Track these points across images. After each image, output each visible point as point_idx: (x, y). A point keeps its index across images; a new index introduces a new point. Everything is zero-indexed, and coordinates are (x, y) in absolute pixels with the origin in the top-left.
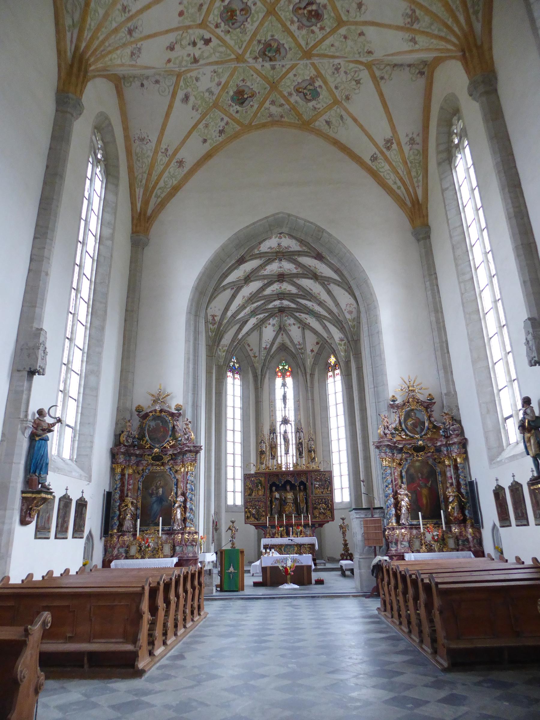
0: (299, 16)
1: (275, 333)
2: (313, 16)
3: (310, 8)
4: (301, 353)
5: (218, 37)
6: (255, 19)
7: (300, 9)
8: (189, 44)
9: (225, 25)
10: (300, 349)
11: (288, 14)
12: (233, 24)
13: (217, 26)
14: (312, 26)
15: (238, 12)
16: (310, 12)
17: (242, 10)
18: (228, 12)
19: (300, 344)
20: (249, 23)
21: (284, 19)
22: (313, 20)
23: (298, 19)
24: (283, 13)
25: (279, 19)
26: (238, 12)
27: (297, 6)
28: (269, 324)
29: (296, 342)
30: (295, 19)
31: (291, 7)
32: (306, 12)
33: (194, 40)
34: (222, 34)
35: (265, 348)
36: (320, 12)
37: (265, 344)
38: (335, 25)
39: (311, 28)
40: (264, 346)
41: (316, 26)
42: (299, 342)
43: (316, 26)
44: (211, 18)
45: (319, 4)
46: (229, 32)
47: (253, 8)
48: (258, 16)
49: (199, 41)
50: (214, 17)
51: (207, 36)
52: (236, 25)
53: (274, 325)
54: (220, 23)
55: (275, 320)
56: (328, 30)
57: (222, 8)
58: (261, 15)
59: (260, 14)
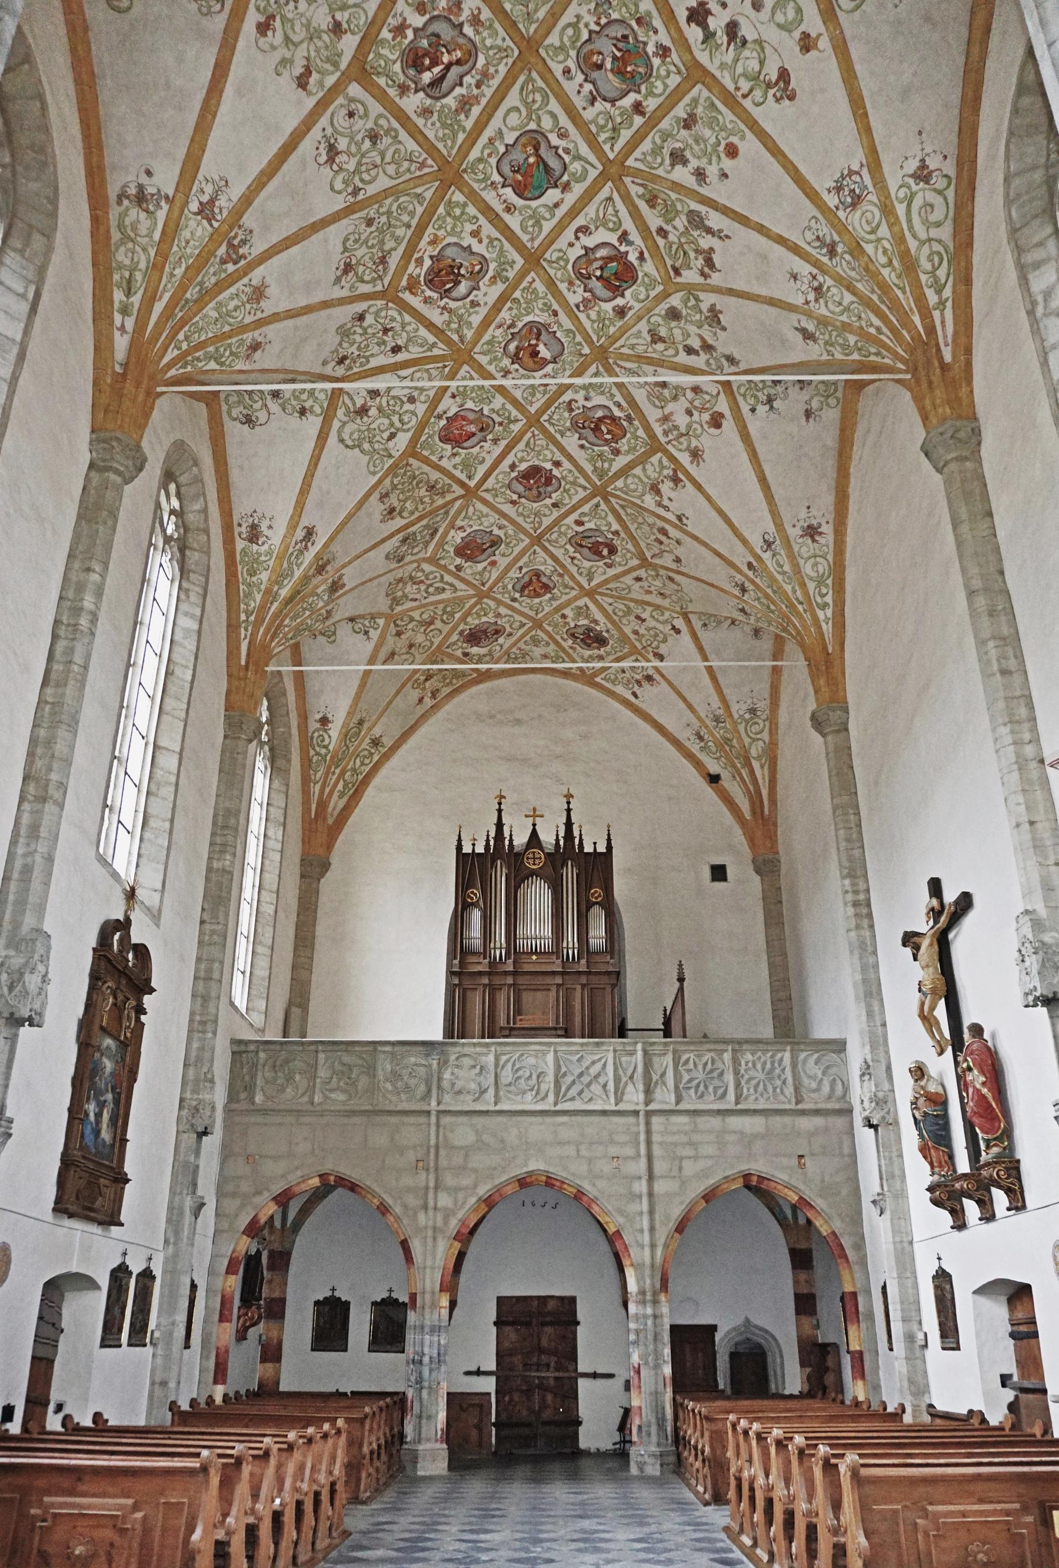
0: (461, 41)
2: (426, 54)
3: (437, 70)
5: (669, 17)
6: (570, 31)
7: (459, 62)
8: (744, 42)
9: (645, 44)
11: (488, 42)
12: (625, 37)
13: (664, 52)
14: (425, 25)
15: (609, 66)
16: (435, 62)
17: (599, 67)
18: (633, 75)
20: (587, 25)
21: (497, 25)
22: (425, 43)
23: (461, 33)
24: (499, 42)
25: (510, 24)
26: (609, 66)
27: (466, 67)
30: (468, 30)
31: (481, 61)
32: (446, 59)
33: (729, 44)
34: (657, 23)
36: (412, 72)
38: (371, 56)
39: (427, 16)
41: (416, 31)
43: (416, 31)
44: (674, 80)
45: (416, 91)
46: (639, 21)
47: (571, 64)
48: (561, 39)
49: (719, 33)
50: (667, 77)
51: (694, 33)
52: (618, 31)
54: (655, 54)
56: (385, 34)
57: (643, 88)
58: (553, 39)
59: (557, 44)
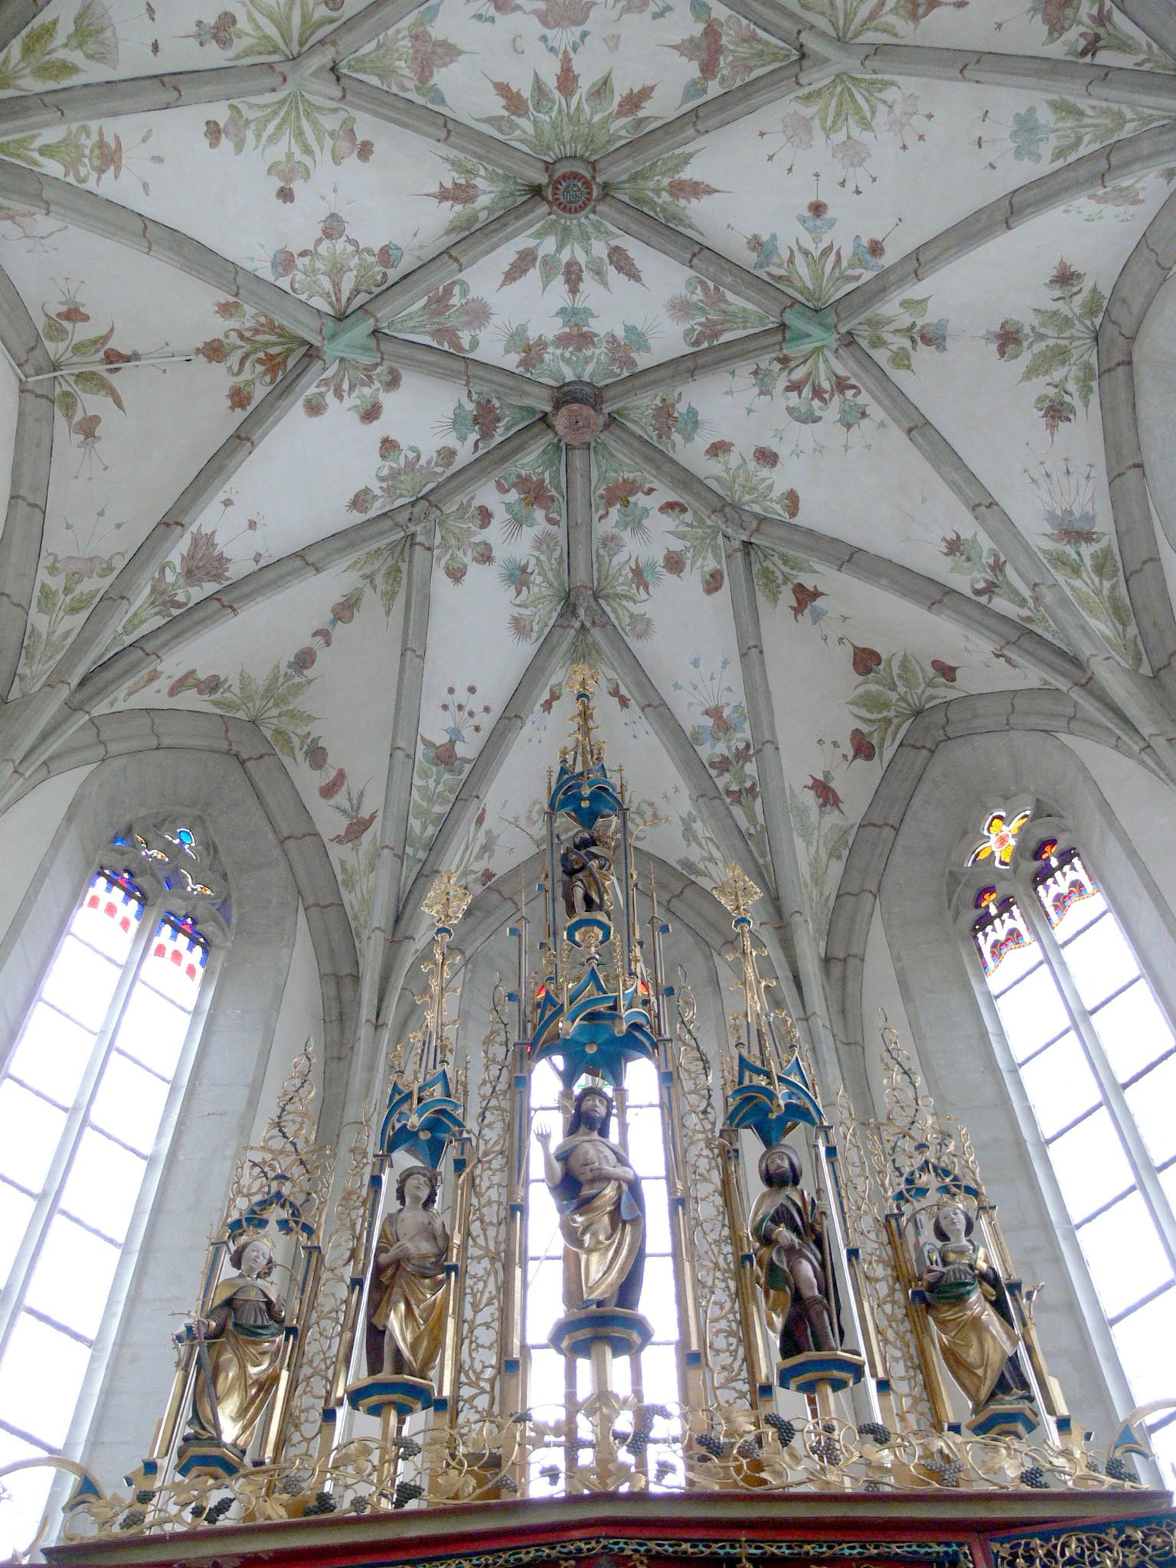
1: (527, 649)
4: (737, 796)
10: (723, 765)
19: (723, 726)
28: (485, 556)
29: (692, 718)
35: (445, 757)
37: (447, 720)
40: (435, 728)
42: (715, 713)
53: (518, 577)
55: (529, 534)
